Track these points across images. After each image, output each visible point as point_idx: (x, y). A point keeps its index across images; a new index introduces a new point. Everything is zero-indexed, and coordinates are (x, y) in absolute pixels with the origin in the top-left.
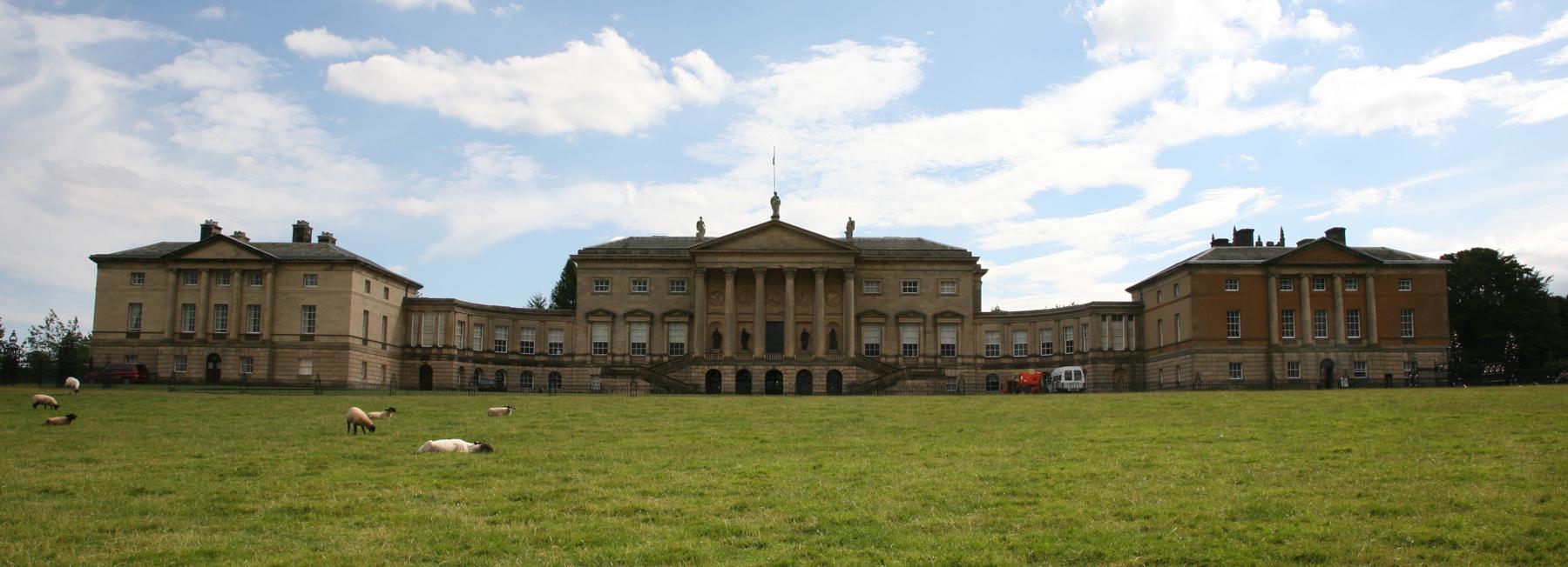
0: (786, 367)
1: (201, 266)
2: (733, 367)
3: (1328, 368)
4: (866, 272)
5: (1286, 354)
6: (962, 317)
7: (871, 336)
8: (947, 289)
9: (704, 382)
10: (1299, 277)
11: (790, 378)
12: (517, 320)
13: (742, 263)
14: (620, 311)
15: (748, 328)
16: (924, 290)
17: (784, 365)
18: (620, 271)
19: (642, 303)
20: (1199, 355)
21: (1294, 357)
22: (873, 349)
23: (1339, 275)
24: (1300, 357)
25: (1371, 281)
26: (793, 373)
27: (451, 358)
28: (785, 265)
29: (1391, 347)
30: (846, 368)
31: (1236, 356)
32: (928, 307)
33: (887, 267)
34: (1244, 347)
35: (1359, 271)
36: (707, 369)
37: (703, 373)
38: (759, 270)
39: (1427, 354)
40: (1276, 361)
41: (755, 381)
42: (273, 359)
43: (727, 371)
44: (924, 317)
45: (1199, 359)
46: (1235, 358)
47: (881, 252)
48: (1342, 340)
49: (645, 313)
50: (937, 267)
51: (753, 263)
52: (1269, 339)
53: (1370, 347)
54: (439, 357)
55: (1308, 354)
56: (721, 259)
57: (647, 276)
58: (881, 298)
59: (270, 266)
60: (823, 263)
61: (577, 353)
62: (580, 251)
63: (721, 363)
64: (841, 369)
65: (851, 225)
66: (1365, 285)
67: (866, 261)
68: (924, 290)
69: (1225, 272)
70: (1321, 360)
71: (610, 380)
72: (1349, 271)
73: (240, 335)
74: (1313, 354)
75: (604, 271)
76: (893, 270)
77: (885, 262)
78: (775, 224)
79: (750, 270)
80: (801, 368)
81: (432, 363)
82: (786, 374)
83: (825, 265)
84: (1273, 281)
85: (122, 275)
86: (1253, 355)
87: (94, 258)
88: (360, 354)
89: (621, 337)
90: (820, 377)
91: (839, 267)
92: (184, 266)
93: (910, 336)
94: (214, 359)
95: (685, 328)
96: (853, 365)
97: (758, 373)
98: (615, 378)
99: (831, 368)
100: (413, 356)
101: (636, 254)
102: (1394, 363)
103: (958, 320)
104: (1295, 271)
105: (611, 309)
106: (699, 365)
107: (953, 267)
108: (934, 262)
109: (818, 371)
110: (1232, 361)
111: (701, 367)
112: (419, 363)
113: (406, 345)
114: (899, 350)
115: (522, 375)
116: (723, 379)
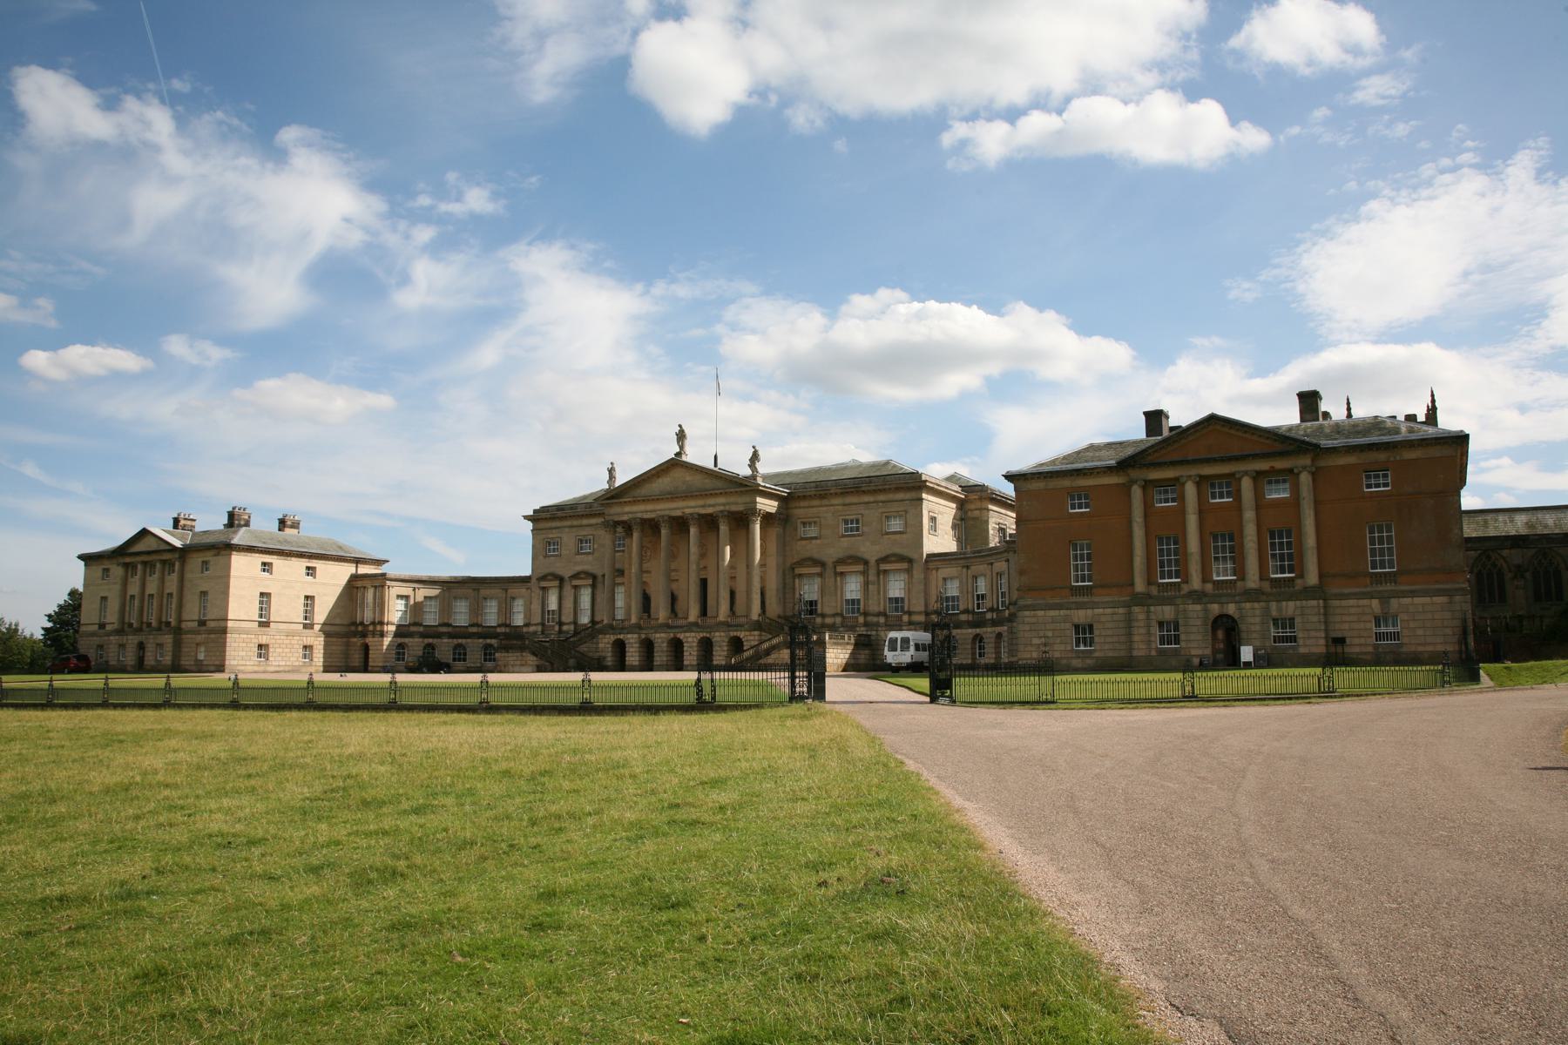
0: (688, 634)
1: (154, 557)
2: (636, 636)
5: (1152, 608)
6: (910, 561)
9: (609, 654)
10: (1176, 482)
11: (690, 647)
12: (478, 590)
13: (647, 512)
14: (567, 574)
15: (674, 586)
16: (865, 529)
17: (685, 632)
18: (567, 530)
19: (586, 563)
20: (1027, 613)
21: (1167, 612)
23: (1246, 473)
24: (1177, 612)
25: (1305, 478)
26: (693, 642)
28: (688, 511)
29: (1346, 591)
30: (747, 633)
31: (1081, 613)
33: (825, 502)
34: (1096, 599)
35: (1280, 464)
36: (613, 638)
37: (608, 643)
38: (720, 515)
39: (1417, 600)
40: (1137, 620)
41: (657, 652)
42: (178, 645)
43: (631, 641)
44: (866, 563)
45: (1027, 620)
46: (1081, 616)
47: (818, 484)
48: (1253, 580)
49: (588, 574)
50: (882, 497)
51: (655, 511)
52: (1132, 585)
53: (1308, 593)
54: (374, 634)
55: (1191, 607)
56: (627, 509)
57: (591, 532)
58: (818, 541)
59: (177, 556)
60: (724, 505)
61: (532, 622)
62: (535, 511)
63: (626, 631)
64: (742, 635)
65: (755, 457)
66: (1181, 498)
67: (799, 497)
68: (865, 529)
69: (1066, 483)
70: (1212, 617)
71: (503, 654)
72: (1263, 465)
73: (142, 623)
74: (1198, 607)
75: (554, 531)
76: (832, 505)
77: (821, 497)
78: (675, 464)
79: (653, 519)
80: (701, 635)
81: (369, 640)
82: (687, 642)
83: (727, 508)
84: (1137, 492)
85: (97, 570)
86: (1109, 611)
87: (81, 557)
88: (253, 636)
90: (720, 647)
91: (741, 508)
92: (128, 560)
93: (852, 588)
94: (141, 646)
95: (860, 579)
96: (755, 630)
97: (661, 639)
98: (508, 652)
99: (732, 634)
100: (355, 634)
101: (580, 510)
102: (1355, 618)
103: (905, 565)
104: (1169, 473)
105: (560, 572)
106: (605, 634)
107: (900, 496)
108: (875, 492)
109: (719, 639)
110: (1076, 621)
111: (608, 636)
115: (425, 648)
116: (627, 649)
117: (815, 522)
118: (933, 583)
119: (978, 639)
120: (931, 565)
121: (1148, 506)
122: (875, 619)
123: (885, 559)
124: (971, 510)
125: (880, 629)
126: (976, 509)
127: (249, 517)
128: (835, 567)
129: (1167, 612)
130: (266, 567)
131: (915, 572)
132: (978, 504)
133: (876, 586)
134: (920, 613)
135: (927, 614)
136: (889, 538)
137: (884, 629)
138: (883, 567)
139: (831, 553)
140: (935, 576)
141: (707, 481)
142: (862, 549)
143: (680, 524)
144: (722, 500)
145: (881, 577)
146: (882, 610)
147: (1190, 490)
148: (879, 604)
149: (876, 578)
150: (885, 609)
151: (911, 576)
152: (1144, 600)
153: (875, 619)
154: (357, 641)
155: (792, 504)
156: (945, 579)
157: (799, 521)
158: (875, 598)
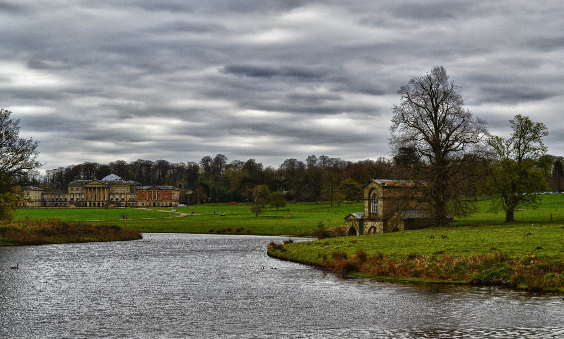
3: (154, 204)
4: (110, 187)
7: (111, 197)
8: (123, 189)
14: (75, 193)
19: (78, 192)
21: (150, 202)
22: (112, 199)
27: (48, 202)
32: (120, 192)
46: (143, 202)
49: (78, 193)
53: (161, 201)
89: (75, 197)
93: (117, 197)
112: (44, 202)
113: (42, 200)
119: (133, 203)
121: (149, 193)
123: (122, 193)
129: (150, 202)
139: (115, 192)
143: (95, 188)
147: (152, 192)
152: (148, 201)
154: (44, 202)
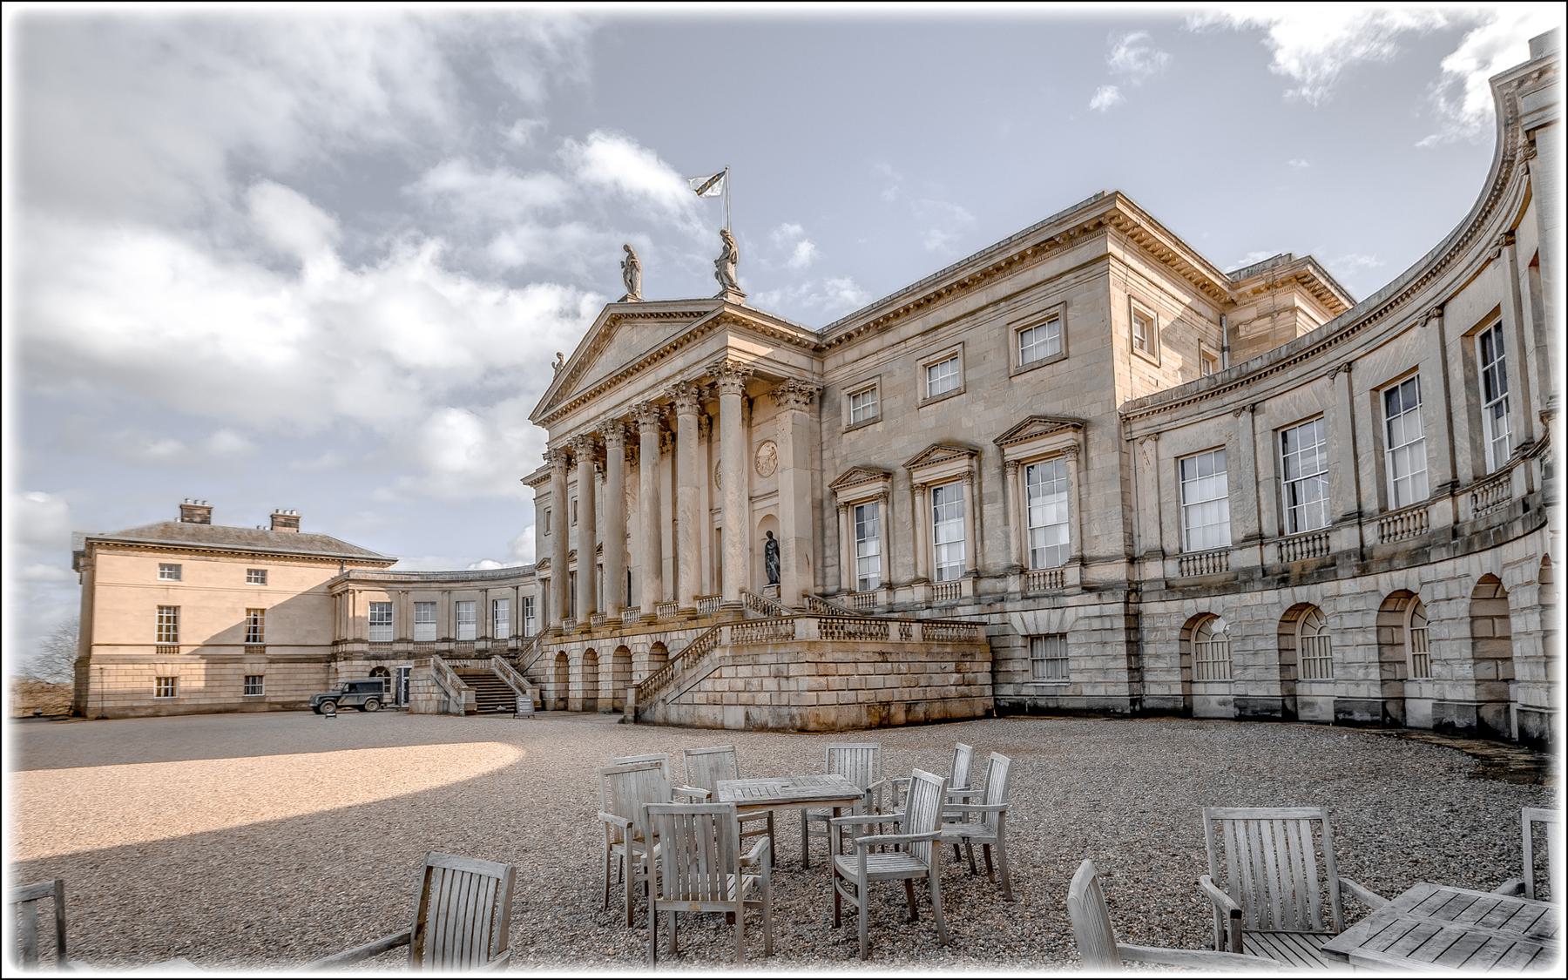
4: (841, 369)
28: (637, 401)
33: (890, 338)
76: (905, 341)
114: (916, 564)
117: (873, 388)
118: (1146, 479)
120: (1138, 428)
122: (999, 585)
124: (1248, 323)
125: (1009, 606)
126: (1259, 317)
127: (209, 512)
128: (911, 477)
130: (174, 571)
131: (1092, 453)
132: (1266, 302)
133: (1000, 505)
134: (1109, 560)
135: (1132, 560)
136: (1027, 382)
137: (1019, 606)
138: (1014, 452)
139: (895, 449)
140: (1151, 455)
141: (660, 332)
142: (967, 423)
144: (678, 362)
145: (1010, 478)
146: (1015, 562)
148: (1008, 547)
149: (998, 488)
150: (1020, 559)
151: (1084, 465)
153: (999, 585)
155: (831, 363)
156: (1181, 461)
157: (844, 393)
158: (999, 533)
